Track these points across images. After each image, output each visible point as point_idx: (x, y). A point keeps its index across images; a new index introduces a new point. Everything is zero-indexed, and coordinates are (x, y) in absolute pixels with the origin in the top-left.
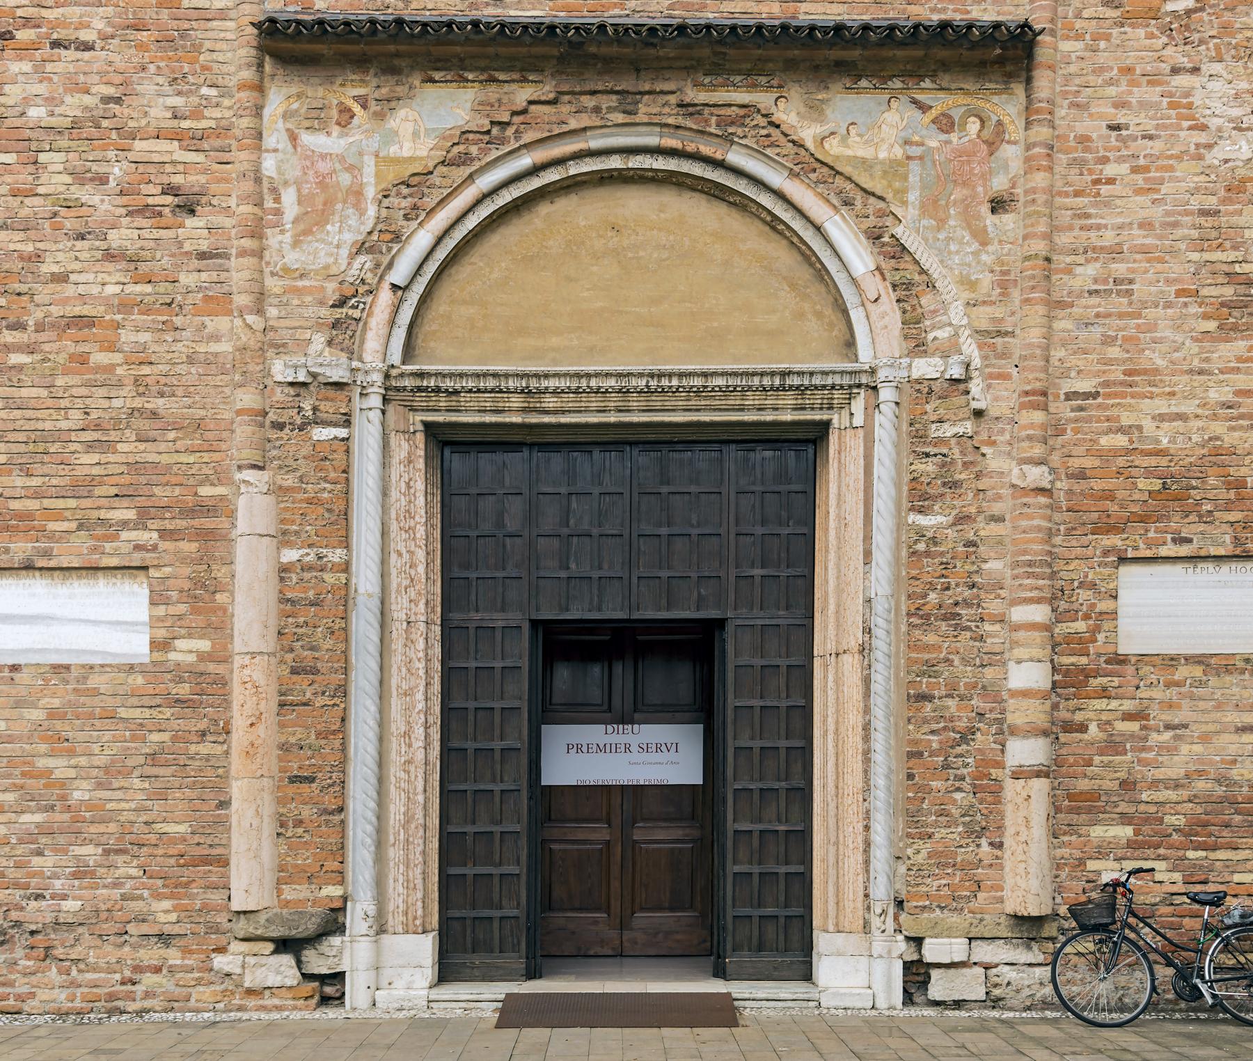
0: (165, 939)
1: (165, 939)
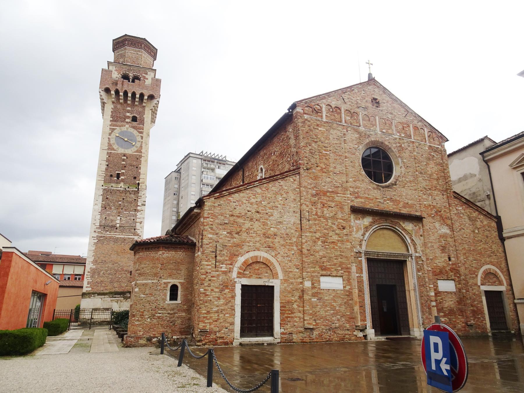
0: (348, 330)
1: (348, 330)
